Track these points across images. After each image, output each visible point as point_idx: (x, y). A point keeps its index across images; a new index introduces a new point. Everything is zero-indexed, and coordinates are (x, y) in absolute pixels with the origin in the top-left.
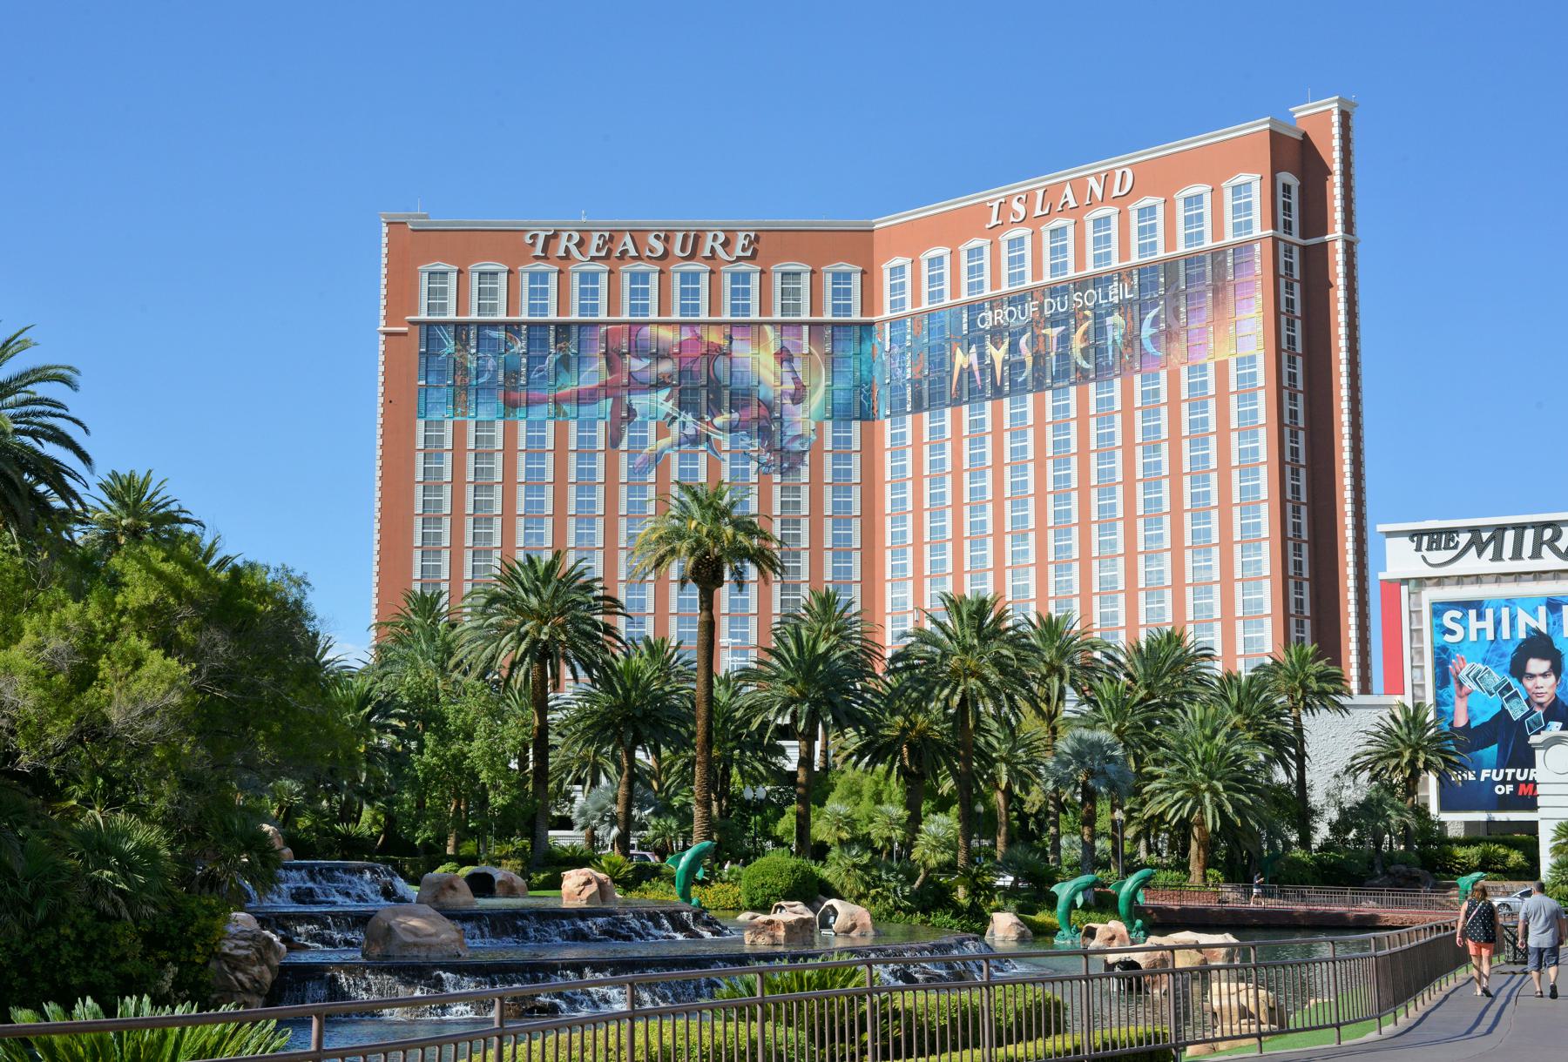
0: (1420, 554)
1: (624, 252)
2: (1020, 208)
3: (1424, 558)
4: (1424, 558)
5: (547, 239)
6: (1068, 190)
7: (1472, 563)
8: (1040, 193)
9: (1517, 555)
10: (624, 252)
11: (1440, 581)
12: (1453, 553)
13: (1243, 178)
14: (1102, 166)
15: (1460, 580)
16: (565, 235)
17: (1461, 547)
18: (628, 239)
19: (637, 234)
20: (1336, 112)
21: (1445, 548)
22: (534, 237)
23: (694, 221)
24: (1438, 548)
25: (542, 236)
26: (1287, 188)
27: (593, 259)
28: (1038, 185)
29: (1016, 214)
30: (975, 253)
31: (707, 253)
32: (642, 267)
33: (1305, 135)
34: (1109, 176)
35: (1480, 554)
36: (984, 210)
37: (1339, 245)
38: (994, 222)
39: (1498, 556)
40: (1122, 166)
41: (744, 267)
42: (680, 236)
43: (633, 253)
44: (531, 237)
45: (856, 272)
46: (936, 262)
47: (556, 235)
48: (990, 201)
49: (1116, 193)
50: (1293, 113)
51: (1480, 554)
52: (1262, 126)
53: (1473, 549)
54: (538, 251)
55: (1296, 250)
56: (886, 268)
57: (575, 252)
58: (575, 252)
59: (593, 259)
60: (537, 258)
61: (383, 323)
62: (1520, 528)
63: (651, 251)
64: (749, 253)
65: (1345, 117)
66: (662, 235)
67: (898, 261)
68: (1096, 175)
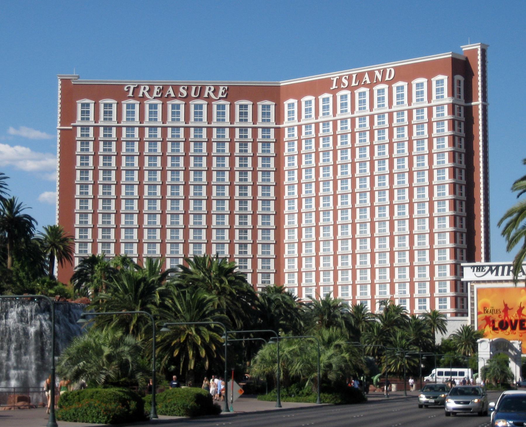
0: (474, 273)
2: (346, 82)
3: (475, 274)
4: (475, 274)
5: (134, 88)
6: (366, 76)
7: (490, 276)
8: (354, 76)
9: (503, 274)
11: (478, 282)
12: (483, 273)
13: (440, 77)
14: (382, 67)
15: (484, 282)
16: (142, 87)
17: (486, 271)
18: (170, 89)
20: (479, 49)
21: (482, 271)
22: (129, 88)
23: (200, 82)
24: (479, 271)
26: (459, 82)
27: (155, 98)
28: (354, 72)
29: (344, 84)
30: (326, 100)
31: (206, 95)
32: (177, 102)
33: (467, 58)
34: (385, 71)
35: (492, 273)
36: (329, 82)
37: (480, 107)
38: (334, 87)
39: (497, 274)
40: (390, 67)
41: (222, 102)
42: (194, 88)
43: (173, 95)
44: (128, 88)
46: (308, 103)
47: (138, 87)
48: (333, 77)
49: (387, 78)
50: (462, 48)
51: (492, 273)
52: (448, 55)
53: (490, 272)
54: (130, 94)
55: (462, 108)
56: (286, 103)
57: (147, 95)
58: (147, 95)
59: (155, 98)
60: (130, 97)
61: (59, 125)
62: (504, 266)
63: (181, 94)
64: (225, 96)
65: (484, 51)
66: (186, 87)
67: (291, 101)
68: (379, 70)
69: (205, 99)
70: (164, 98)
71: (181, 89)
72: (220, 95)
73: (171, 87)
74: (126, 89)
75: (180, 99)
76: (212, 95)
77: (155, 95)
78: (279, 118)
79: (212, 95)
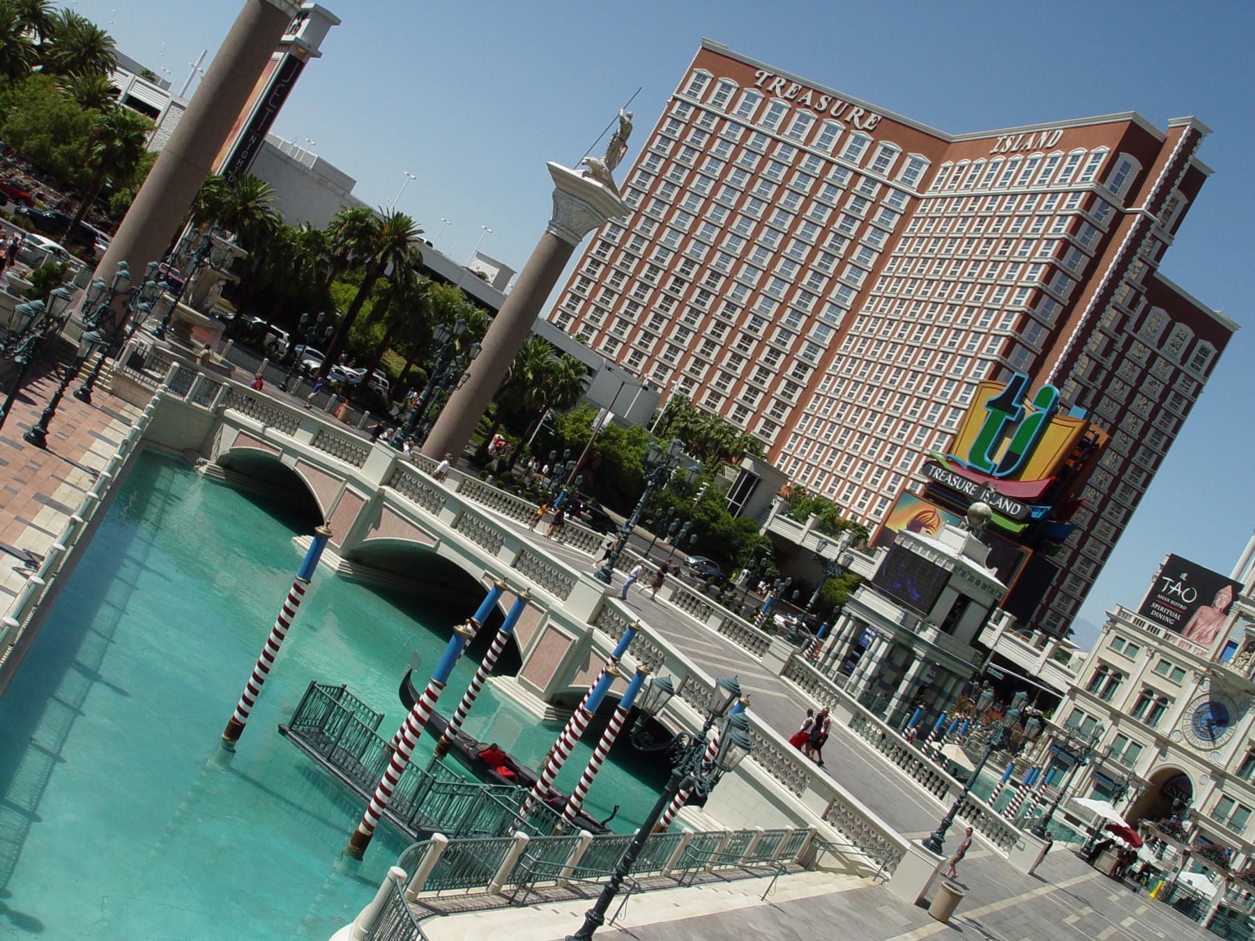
1: (804, 101)
5: (768, 77)
10: (804, 101)
16: (778, 79)
19: (818, 93)
22: (762, 74)
25: (766, 74)
27: (786, 98)
31: (848, 119)
32: (809, 113)
41: (864, 135)
42: (839, 103)
43: (808, 103)
45: (927, 163)
56: (943, 165)
57: (778, 91)
58: (778, 91)
59: (786, 98)
60: (756, 86)
69: (846, 122)
70: (796, 102)
71: (822, 100)
72: (866, 125)
73: (811, 92)
74: (757, 75)
75: (815, 110)
76: (856, 121)
77: (787, 95)
78: (923, 186)
79: (856, 121)
